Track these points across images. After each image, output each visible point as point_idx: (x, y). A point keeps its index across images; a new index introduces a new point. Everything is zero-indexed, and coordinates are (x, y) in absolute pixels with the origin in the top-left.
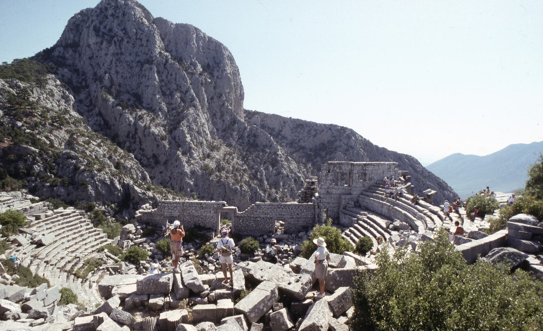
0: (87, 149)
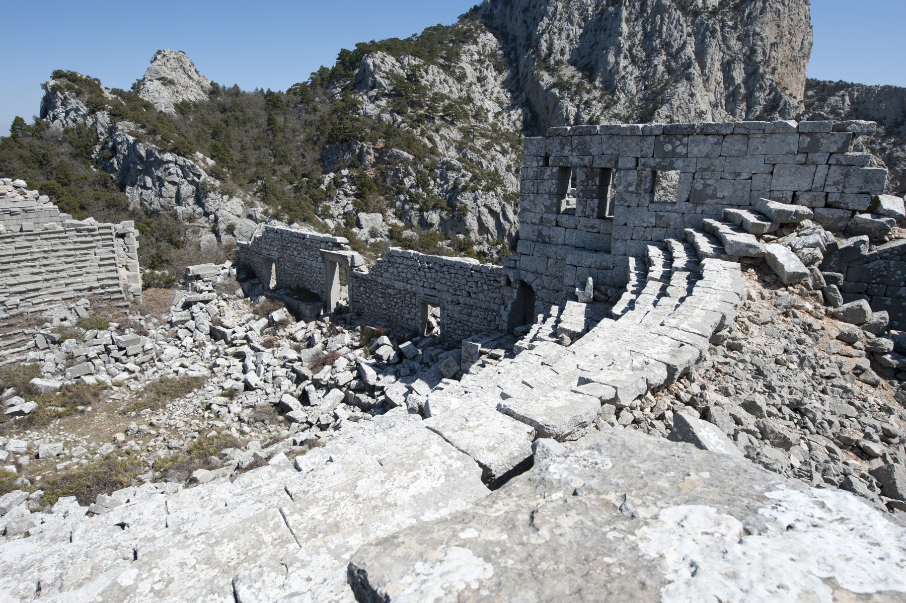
0: (483, 156)
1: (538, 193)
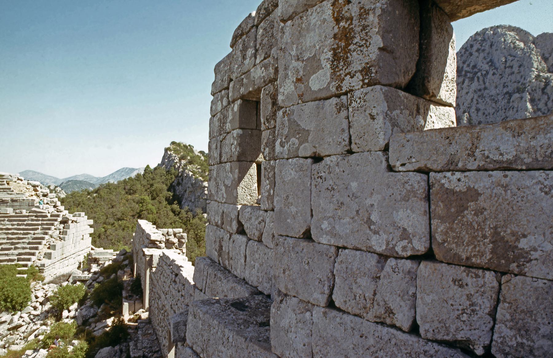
1: (221, 163)
